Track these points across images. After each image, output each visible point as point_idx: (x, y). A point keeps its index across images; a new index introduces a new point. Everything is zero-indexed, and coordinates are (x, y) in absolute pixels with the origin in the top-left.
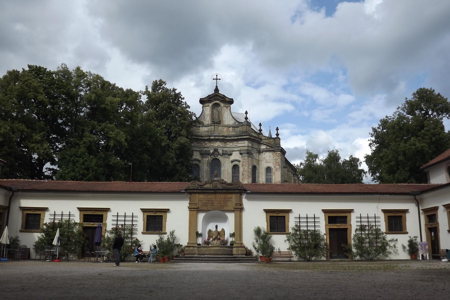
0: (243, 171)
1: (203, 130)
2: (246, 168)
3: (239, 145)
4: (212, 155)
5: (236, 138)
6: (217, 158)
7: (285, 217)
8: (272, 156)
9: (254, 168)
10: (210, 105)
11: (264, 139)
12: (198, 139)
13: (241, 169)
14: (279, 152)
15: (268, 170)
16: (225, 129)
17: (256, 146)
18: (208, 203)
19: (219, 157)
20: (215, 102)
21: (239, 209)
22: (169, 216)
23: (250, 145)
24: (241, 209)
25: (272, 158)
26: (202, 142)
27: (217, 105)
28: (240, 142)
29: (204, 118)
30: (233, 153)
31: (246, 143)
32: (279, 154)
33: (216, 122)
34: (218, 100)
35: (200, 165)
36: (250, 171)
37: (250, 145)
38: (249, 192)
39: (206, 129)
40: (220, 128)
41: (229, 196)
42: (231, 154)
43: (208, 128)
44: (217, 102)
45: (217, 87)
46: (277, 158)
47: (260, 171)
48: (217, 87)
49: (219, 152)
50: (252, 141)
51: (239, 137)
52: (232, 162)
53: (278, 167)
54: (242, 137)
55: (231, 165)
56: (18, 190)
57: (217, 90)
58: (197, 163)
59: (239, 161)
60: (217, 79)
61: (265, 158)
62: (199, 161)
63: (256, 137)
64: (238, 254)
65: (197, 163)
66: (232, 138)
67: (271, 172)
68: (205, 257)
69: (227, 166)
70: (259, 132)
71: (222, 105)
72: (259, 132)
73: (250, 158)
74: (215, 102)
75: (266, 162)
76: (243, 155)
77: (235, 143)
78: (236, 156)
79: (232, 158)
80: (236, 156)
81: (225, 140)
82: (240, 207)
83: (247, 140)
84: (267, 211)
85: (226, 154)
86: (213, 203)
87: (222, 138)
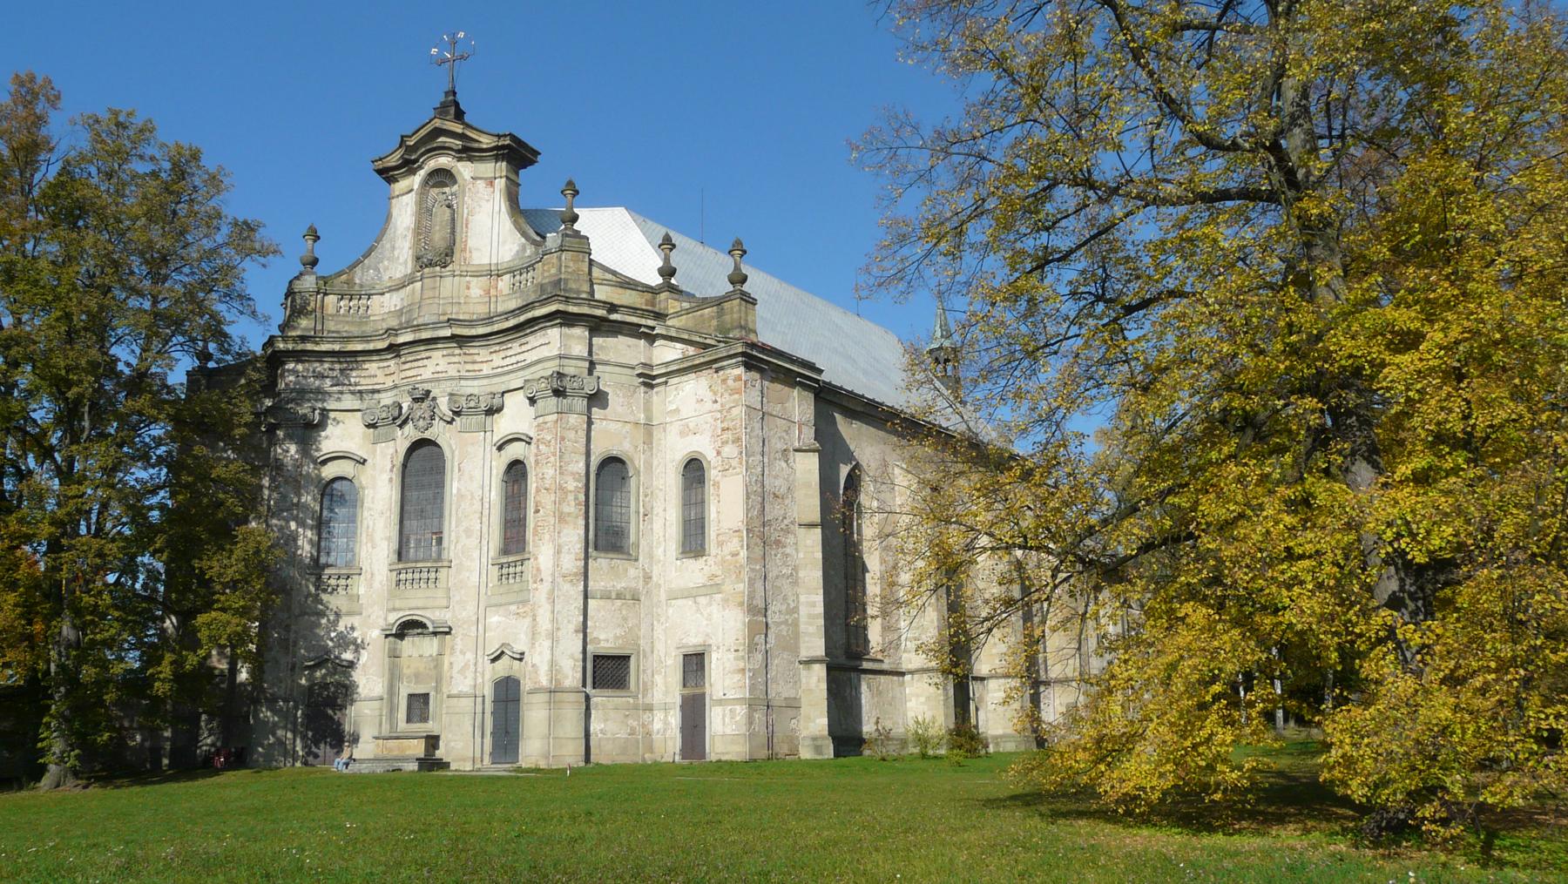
0: (538, 490)
2: (550, 472)
3: (531, 357)
6: (427, 435)
8: (709, 396)
9: (612, 470)
10: (417, 180)
11: (677, 314)
15: (694, 470)
16: (476, 288)
19: (439, 432)
20: (433, 164)
25: (709, 405)
27: (442, 177)
28: (534, 340)
29: (393, 248)
32: (738, 378)
34: (444, 149)
39: (392, 302)
40: (448, 286)
43: (403, 293)
44: (444, 161)
47: (658, 483)
51: (522, 318)
53: (730, 450)
54: (529, 315)
55: (501, 462)
61: (677, 410)
63: (634, 310)
66: (496, 328)
69: (477, 474)
70: (656, 280)
71: (465, 170)
72: (656, 280)
74: (433, 164)
75: (682, 434)
77: (515, 347)
78: (516, 416)
79: (504, 425)
80: (516, 416)
85: (473, 411)
87: (447, 333)
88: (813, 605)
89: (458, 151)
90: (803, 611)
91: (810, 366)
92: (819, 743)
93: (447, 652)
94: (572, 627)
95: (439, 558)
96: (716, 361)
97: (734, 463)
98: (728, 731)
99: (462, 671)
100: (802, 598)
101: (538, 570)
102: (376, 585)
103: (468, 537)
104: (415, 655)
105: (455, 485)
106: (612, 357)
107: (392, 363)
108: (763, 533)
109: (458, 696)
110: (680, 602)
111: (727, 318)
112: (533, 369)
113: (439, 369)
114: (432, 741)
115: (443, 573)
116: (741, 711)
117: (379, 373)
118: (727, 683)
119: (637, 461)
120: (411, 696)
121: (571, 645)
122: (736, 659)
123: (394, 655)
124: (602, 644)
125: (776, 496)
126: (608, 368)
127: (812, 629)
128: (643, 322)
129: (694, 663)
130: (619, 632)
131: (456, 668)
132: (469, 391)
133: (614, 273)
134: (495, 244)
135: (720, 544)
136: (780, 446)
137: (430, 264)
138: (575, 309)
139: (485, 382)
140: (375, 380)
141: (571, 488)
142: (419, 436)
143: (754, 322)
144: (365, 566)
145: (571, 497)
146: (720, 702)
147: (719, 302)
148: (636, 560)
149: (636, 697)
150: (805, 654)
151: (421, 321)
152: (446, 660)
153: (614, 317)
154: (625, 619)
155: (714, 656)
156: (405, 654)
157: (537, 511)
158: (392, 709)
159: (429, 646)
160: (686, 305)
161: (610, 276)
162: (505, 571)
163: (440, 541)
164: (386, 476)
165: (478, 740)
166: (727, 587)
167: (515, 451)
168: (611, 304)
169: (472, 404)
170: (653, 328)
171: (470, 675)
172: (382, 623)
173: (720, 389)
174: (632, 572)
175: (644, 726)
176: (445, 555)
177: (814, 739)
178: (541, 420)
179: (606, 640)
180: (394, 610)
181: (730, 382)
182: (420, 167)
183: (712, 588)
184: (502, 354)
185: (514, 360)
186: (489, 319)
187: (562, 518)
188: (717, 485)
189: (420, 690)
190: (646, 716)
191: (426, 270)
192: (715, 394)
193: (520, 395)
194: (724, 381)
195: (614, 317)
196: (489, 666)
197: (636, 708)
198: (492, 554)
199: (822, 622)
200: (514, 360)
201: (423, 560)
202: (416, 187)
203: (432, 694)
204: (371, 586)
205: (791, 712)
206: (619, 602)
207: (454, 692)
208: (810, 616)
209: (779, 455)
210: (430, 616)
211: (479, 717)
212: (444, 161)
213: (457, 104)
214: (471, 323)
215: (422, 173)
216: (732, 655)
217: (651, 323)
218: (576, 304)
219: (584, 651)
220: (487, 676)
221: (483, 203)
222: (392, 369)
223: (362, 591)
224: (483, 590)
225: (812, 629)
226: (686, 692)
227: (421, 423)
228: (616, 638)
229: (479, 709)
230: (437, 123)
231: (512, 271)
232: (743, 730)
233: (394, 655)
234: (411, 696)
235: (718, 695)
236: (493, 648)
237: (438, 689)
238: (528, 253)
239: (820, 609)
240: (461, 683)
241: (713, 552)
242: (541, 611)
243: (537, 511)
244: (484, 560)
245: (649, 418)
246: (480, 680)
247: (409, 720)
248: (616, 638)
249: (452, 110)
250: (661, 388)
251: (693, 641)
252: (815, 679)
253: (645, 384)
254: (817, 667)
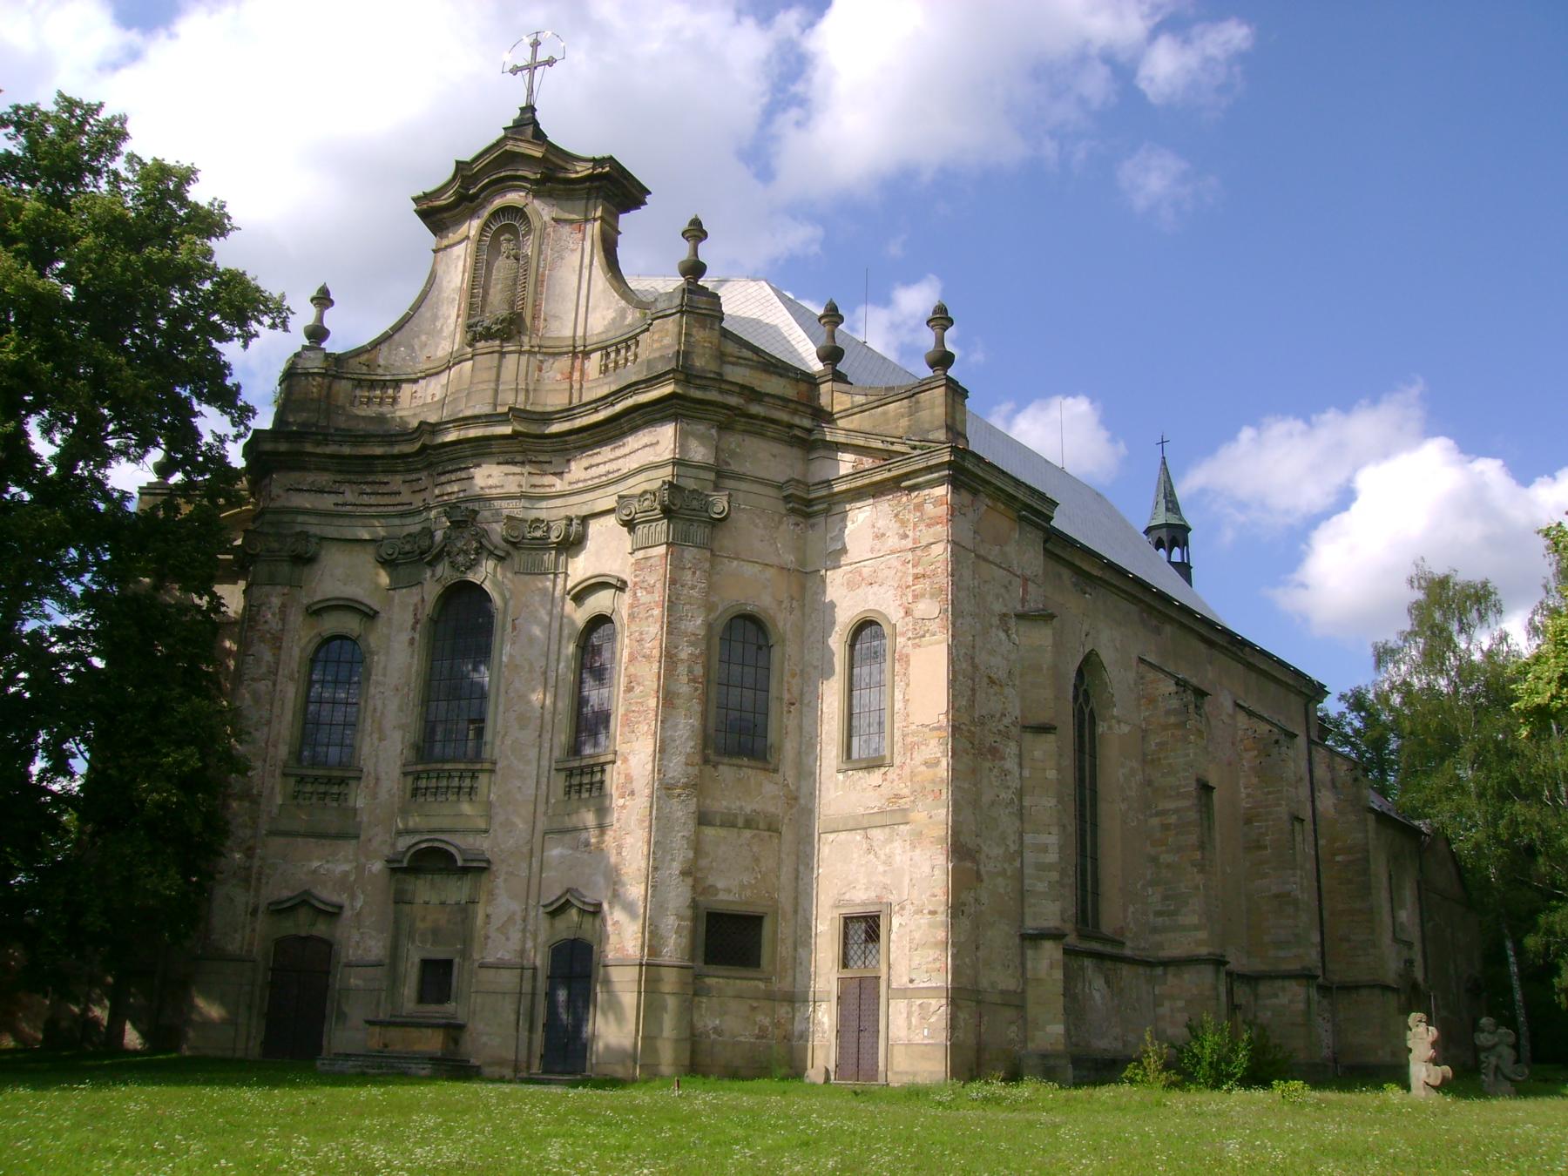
1: (418, 402)
4: (438, 557)
10: (473, 227)
11: (848, 413)
12: (366, 465)
13: (624, 647)
14: (941, 491)
17: (767, 460)
19: (486, 574)
20: (498, 202)
23: (699, 453)
25: (893, 541)
26: (396, 482)
28: (633, 442)
29: (435, 318)
30: (594, 527)
31: (661, 442)
32: (937, 502)
33: (501, 328)
35: (373, 641)
36: (685, 652)
37: (699, 453)
39: (433, 389)
42: (572, 544)
43: (443, 378)
44: (514, 198)
45: (529, 109)
46: (927, 535)
48: (529, 109)
49: (481, 536)
50: (724, 427)
51: (619, 407)
53: (929, 608)
54: (629, 402)
58: (349, 624)
59: (621, 586)
60: (532, 67)
62: (370, 615)
65: (349, 624)
66: (578, 423)
67: (876, 656)
70: (816, 366)
71: (542, 211)
72: (816, 366)
73: (690, 554)
74: (498, 202)
75: (851, 585)
76: (641, 530)
77: (606, 452)
79: (580, 568)
81: (539, 441)
83: (674, 418)
88: (1044, 849)
89: (536, 182)
90: (1029, 857)
91: (1042, 496)
92: (1052, 1062)
93: (483, 898)
94: (676, 867)
95: (478, 757)
96: (907, 476)
97: (934, 626)
98: (917, 1039)
99: (503, 929)
100: (1028, 838)
101: (629, 778)
102: (383, 795)
103: (522, 728)
104: (435, 900)
105: (507, 648)
106: (747, 468)
107: (423, 475)
108: (972, 736)
109: (498, 966)
110: (843, 835)
111: (924, 415)
112: (631, 482)
113: (491, 482)
114: (454, 1030)
115: (483, 779)
116: (938, 1009)
117: (404, 489)
118: (916, 960)
119: (783, 622)
120: (426, 964)
121: (678, 895)
122: (931, 925)
123: (400, 899)
124: (722, 896)
125: (992, 681)
126: (743, 486)
127: (1041, 887)
128: (797, 420)
129: (865, 929)
130: (746, 878)
131: (496, 922)
132: (534, 514)
133: (756, 350)
134: (582, 310)
135: (910, 748)
136: (998, 607)
137: (488, 335)
138: (698, 394)
139: (558, 502)
140: (398, 499)
141: (684, 655)
143: (964, 422)
144: (368, 765)
145: (682, 669)
146: (904, 993)
147: (914, 392)
148: (776, 771)
149: (768, 980)
150: (1031, 924)
151: (468, 413)
152: (481, 911)
153: (755, 409)
154: (757, 860)
155: (896, 921)
156: (419, 900)
157: (629, 689)
158: (395, 979)
159: (457, 890)
160: (860, 399)
161: (748, 354)
162: (575, 781)
163: (480, 733)
164: (405, 637)
165: (524, 1034)
166: (919, 816)
168: (752, 390)
169: (538, 534)
170: (810, 431)
171: (515, 936)
172: (387, 851)
173: (912, 517)
174: (770, 788)
175: (777, 1025)
176: (486, 753)
177: (1044, 1056)
178: (640, 554)
179: (732, 889)
180: (408, 832)
181: (929, 507)
182: (482, 206)
183: (893, 816)
184: (585, 462)
185: (602, 469)
186: (568, 413)
187: (668, 699)
188: (906, 659)
189: (439, 953)
190: (783, 1010)
191: (481, 344)
192: (903, 523)
193: (611, 520)
194: (919, 507)
195: (755, 409)
196: (544, 923)
197: (770, 997)
198: (557, 753)
199: (1055, 876)
200: (602, 469)
201: (454, 760)
202: (472, 233)
203: (457, 960)
204: (375, 796)
205: (1010, 1013)
206: (748, 833)
207: (490, 959)
208: (1041, 867)
209: (995, 621)
210: (460, 844)
211: (526, 1002)
212: (514, 198)
213: (536, 124)
214: (547, 418)
215: (486, 213)
216: (924, 920)
217: (807, 423)
218: (699, 387)
219: (694, 904)
220: (542, 938)
221: (566, 254)
222: (423, 484)
223: (360, 803)
224: (541, 808)
225: (1041, 887)
226: (848, 973)
227: (461, 559)
228: (743, 887)
229: (527, 987)
230: (510, 146)
231: (605, 349)
232: (942, 1037)
233: (400, 899)
234: (426, 964)
235: (900, 979)
236: (553, 893)
237: (465, 954)
238: (629, 320)
239: (1052, 857)
240: (501, 947)
241: (897, 762)
242: (629, 840)
243: (629, 689)
244: (545, 763)
245: (802, 562)
246: (529, 944)
247: (422, 999)
248: (743, 887)
249: (530, 130)
250: (820, 520)
251: (861, 897)
252: (1044, 964)
253: (793, 511)
254: (1048, 945)
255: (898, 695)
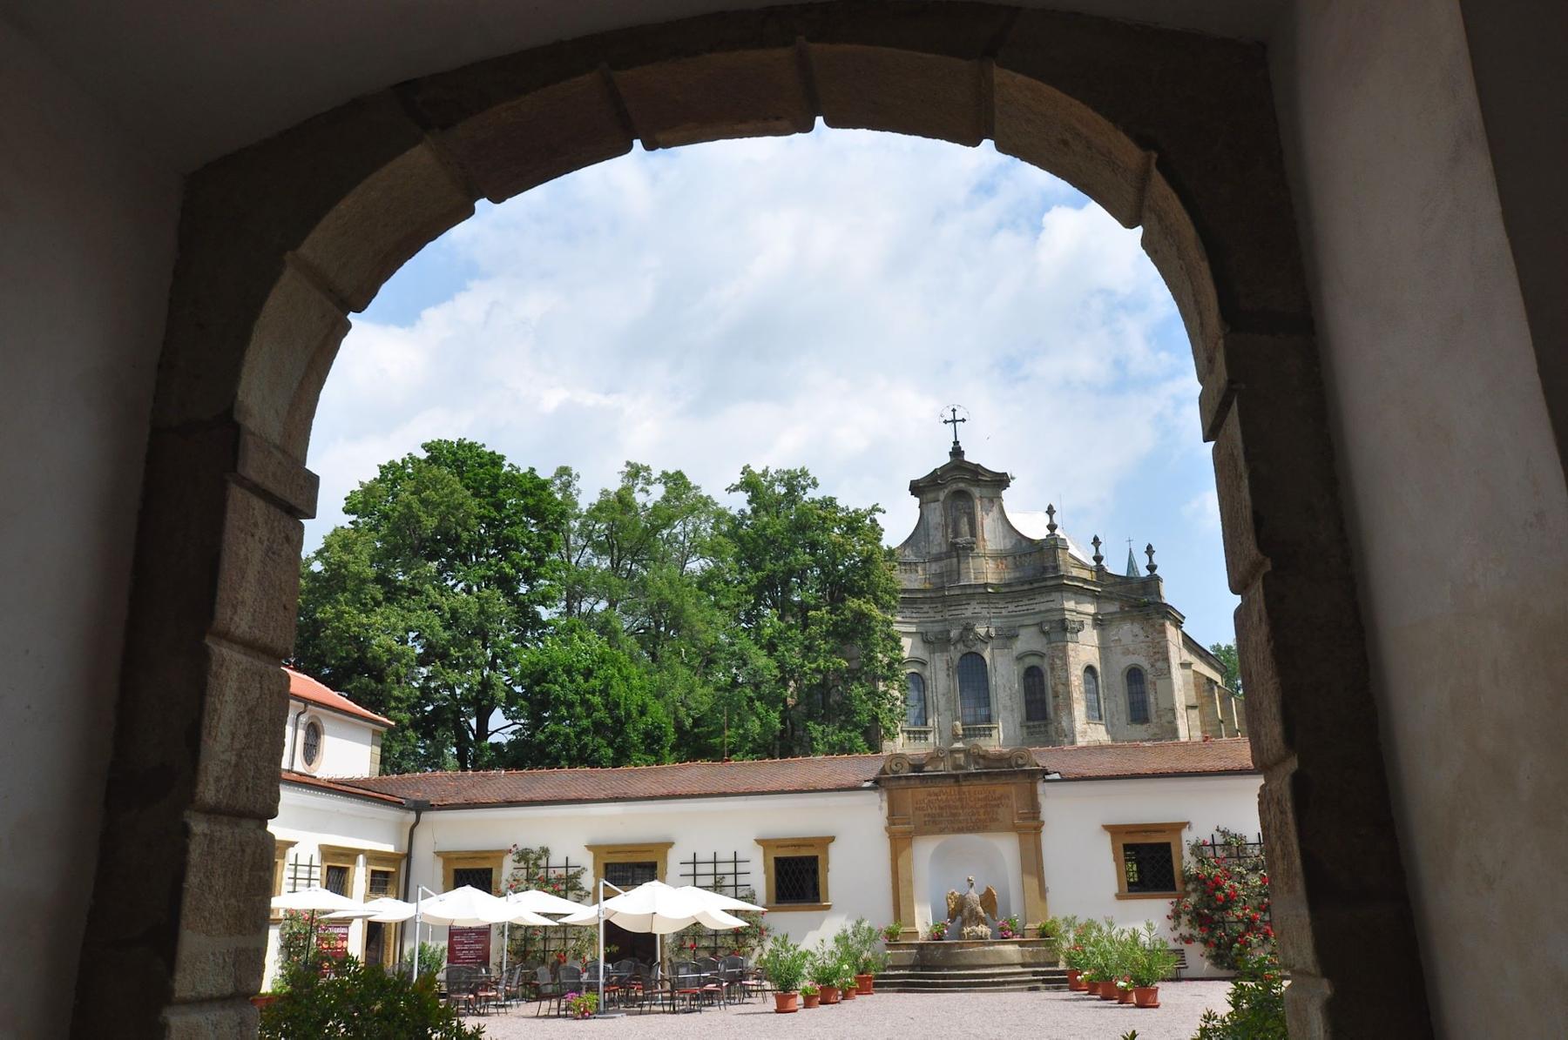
3: (1037, 608)
5: (1026, 587)
7: (1168, 845)
8: (1141, 634)
18: (941, 815)
19: (978, 648)
21: (1030, 826)
22: (834, 850)
24: (1038, 829)
25: (1142, 638)
26: (926, 607)
30: (1023, 633)
34: (962, 480)
35: (927, 674)
38: (1057, 776)
41: (999, 789)
43: (942, 563)
44: (962, 485)
45: (956, 443)
48: (956, 443)
52: (1020, 658)
56: (431, 808)
57: (957, 452)
59: (1041, 656)
60: (954, 421)
63: (1085, 581)
64: (1039, 965)
68: (944, 977)
71: (976, 492)
74: (955, 487)
76: (1053, 637)
79: (1020, 646)
82: (1034, 823)
84: (1114, 830)
86: (954, 815)
142: (966, 650)
167: (1034, 661)
255: (1152, 699)
